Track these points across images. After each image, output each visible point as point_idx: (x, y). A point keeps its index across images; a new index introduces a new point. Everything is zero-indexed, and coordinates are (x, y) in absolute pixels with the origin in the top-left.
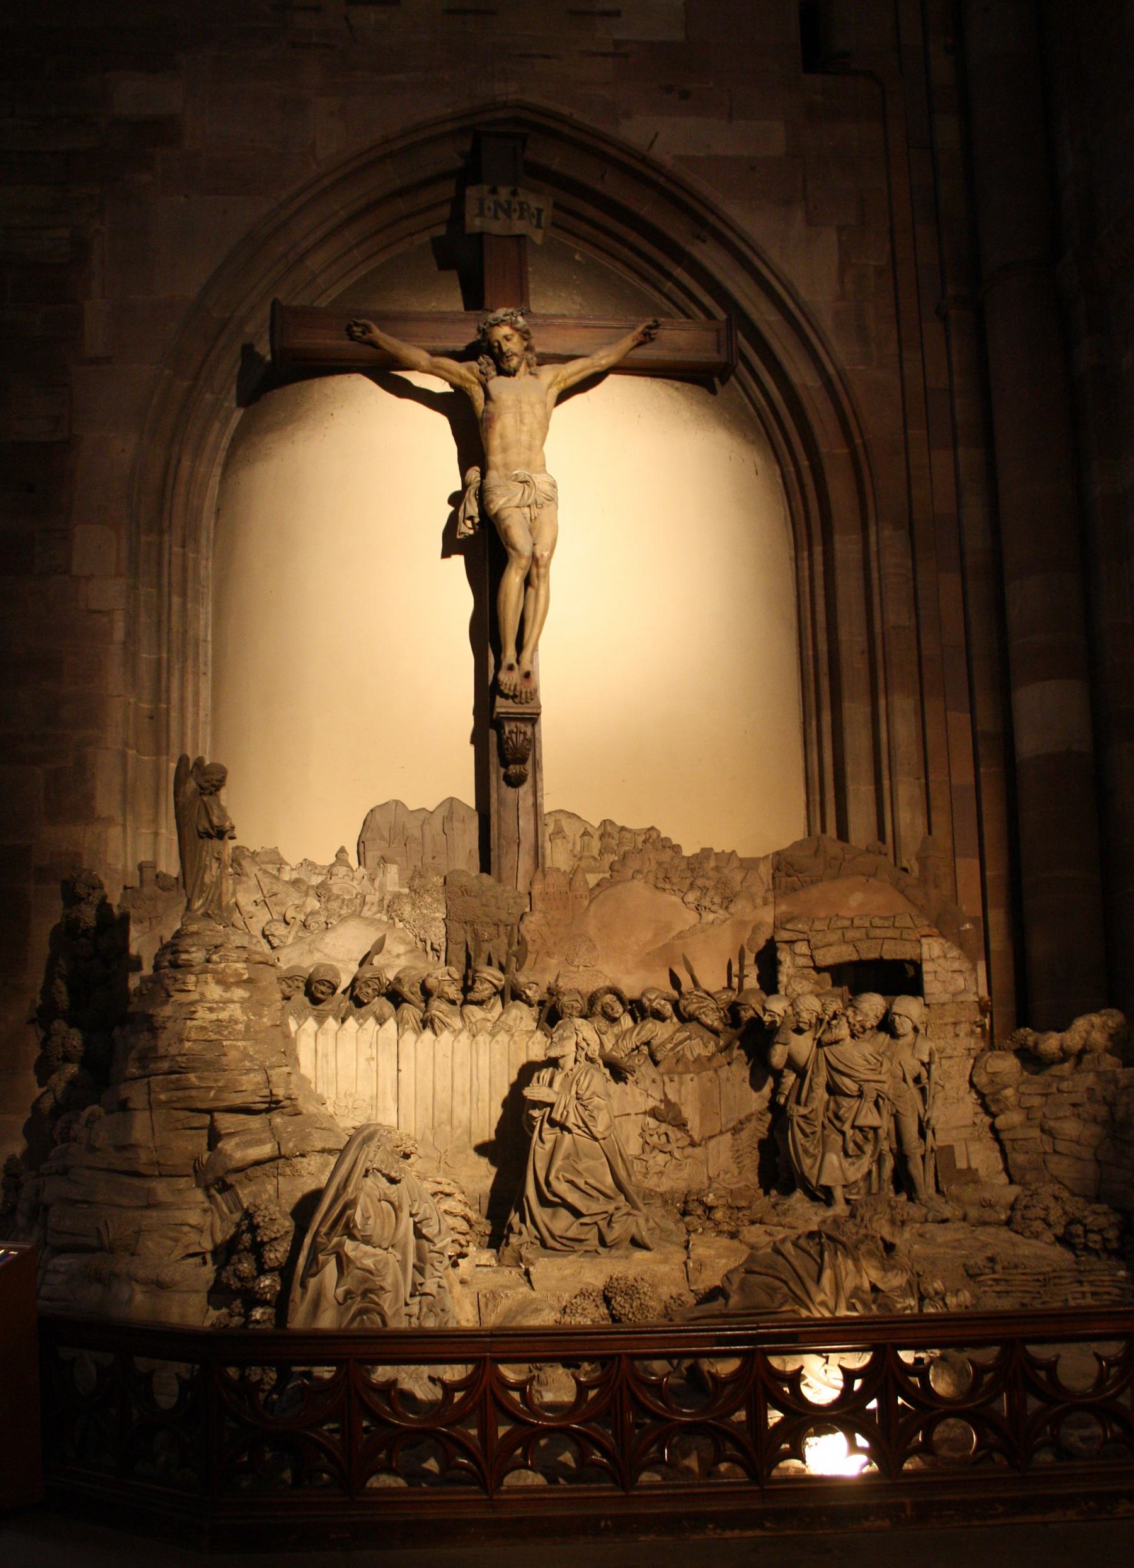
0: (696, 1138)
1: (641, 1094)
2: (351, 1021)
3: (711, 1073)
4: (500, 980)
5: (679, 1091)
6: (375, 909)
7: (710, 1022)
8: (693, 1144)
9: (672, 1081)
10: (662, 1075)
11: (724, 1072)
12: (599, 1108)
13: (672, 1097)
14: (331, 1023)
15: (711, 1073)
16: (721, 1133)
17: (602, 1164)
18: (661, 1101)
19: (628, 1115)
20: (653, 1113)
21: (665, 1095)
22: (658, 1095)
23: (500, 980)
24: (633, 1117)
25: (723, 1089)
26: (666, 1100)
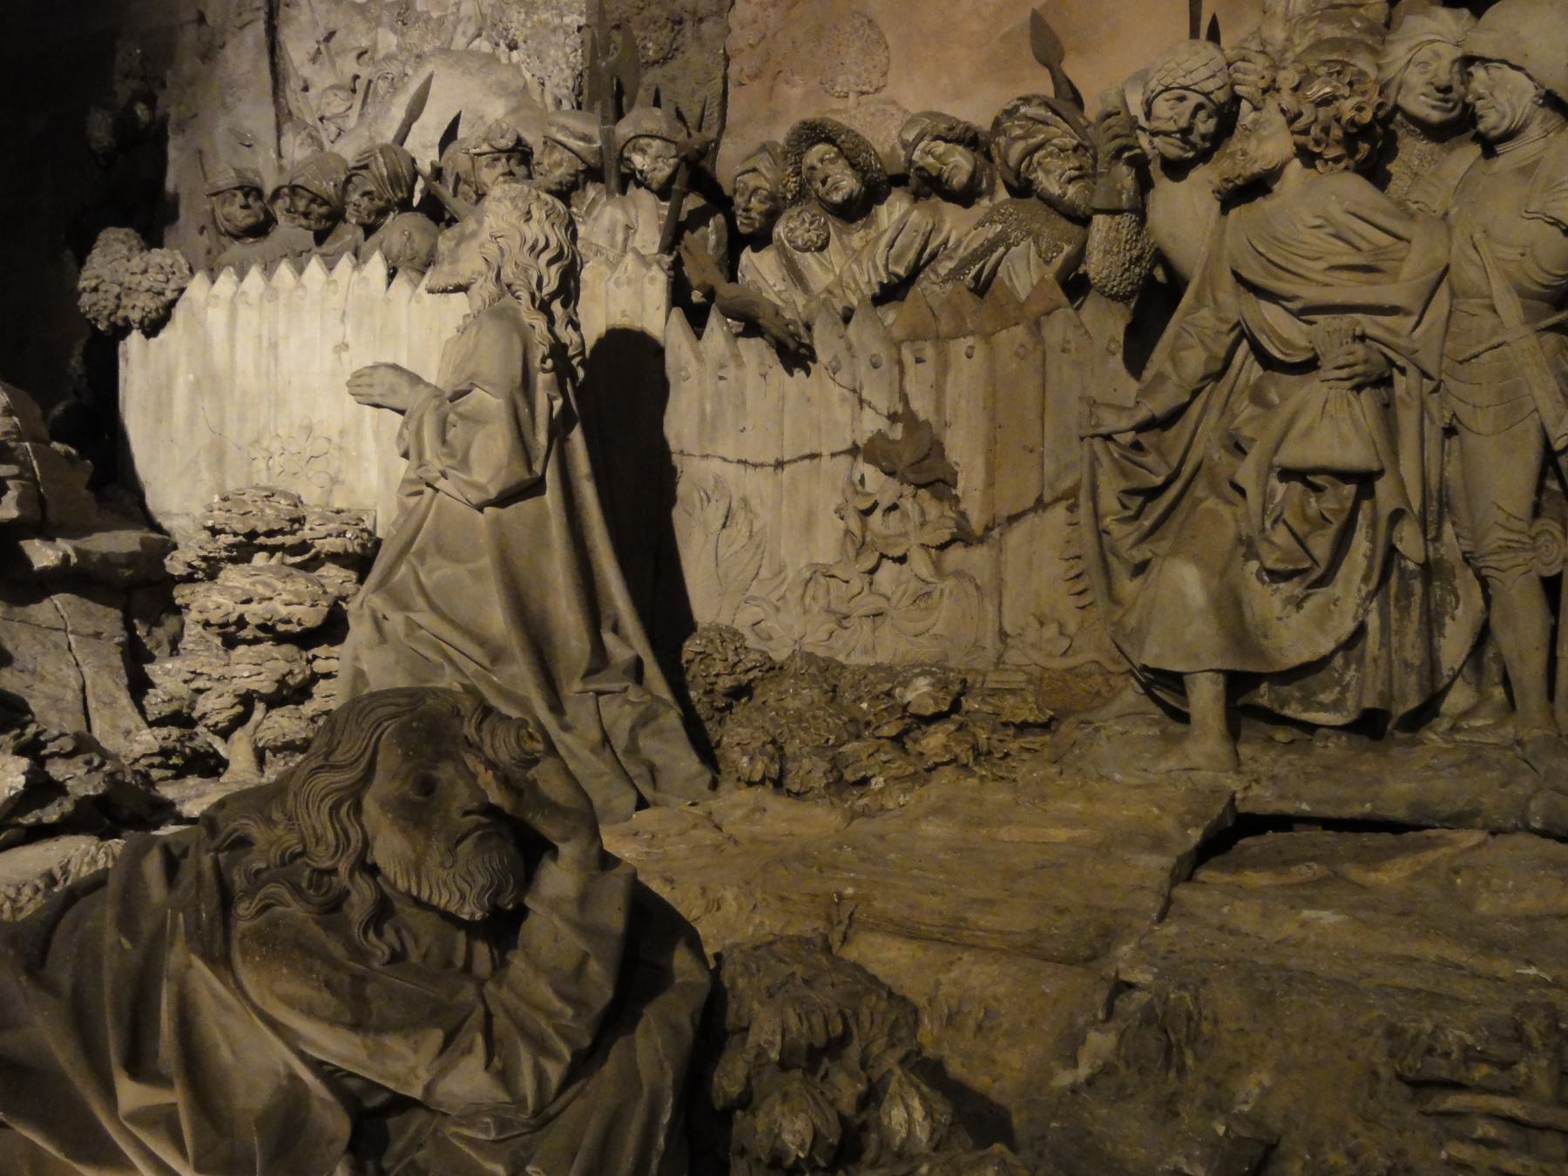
0: (976, 520)
1: (843, 400)
2: (315, 268)
3: (1020, 332)
4: (586, 138)
5: (939, 389)
6: (472, 30)
7: (1055, 190)
8: (963, 537)
9: (919, 361)
10: (898, 345)
11: (1057, 329)
12: (475, 420)
13: (922, 406)
14: (284, 271)
15: (1020, 332)
16: (1040, 505)
17: (477, 575)
18: (893, 418)
19: (813, 456)
20: (871, 451)
21: (904, 398)
22: (882, 400)
23: (586, 138)
24: (825, 461)
25: (1053, 376)
26: (903, 416)
